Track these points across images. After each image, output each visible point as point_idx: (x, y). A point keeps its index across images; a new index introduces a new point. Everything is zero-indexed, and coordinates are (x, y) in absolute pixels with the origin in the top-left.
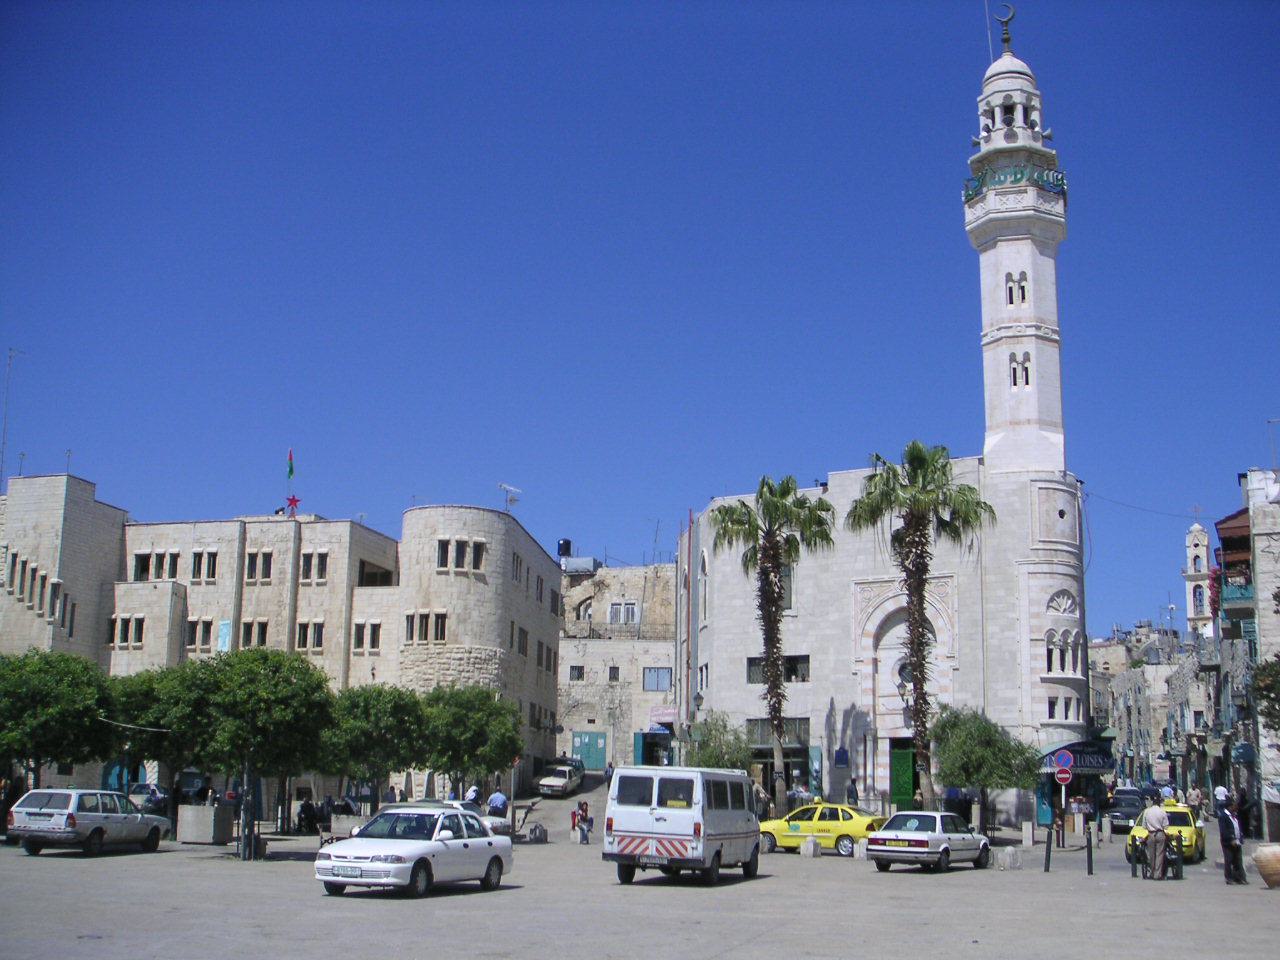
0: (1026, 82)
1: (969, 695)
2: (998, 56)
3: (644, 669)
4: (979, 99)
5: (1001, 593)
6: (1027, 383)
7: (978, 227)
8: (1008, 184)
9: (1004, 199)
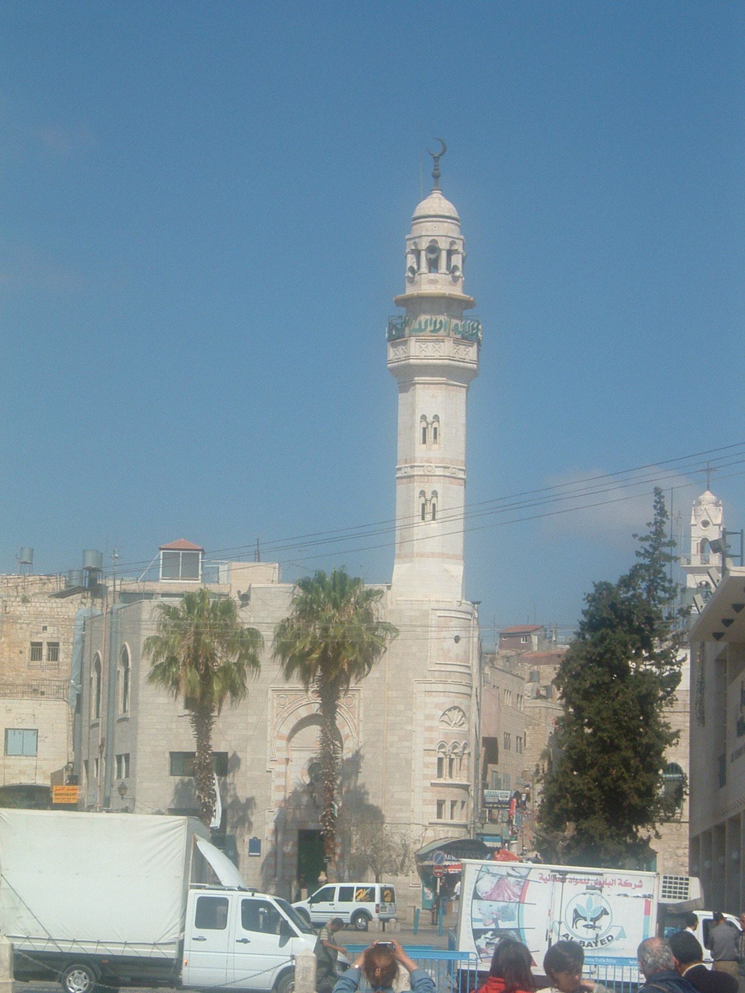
0: (453, 227)
2: (427, 194)
3: (7, 730)
4: (407, 237)
5: (401, 707)
7: (397, 368)
8: (427, 333)
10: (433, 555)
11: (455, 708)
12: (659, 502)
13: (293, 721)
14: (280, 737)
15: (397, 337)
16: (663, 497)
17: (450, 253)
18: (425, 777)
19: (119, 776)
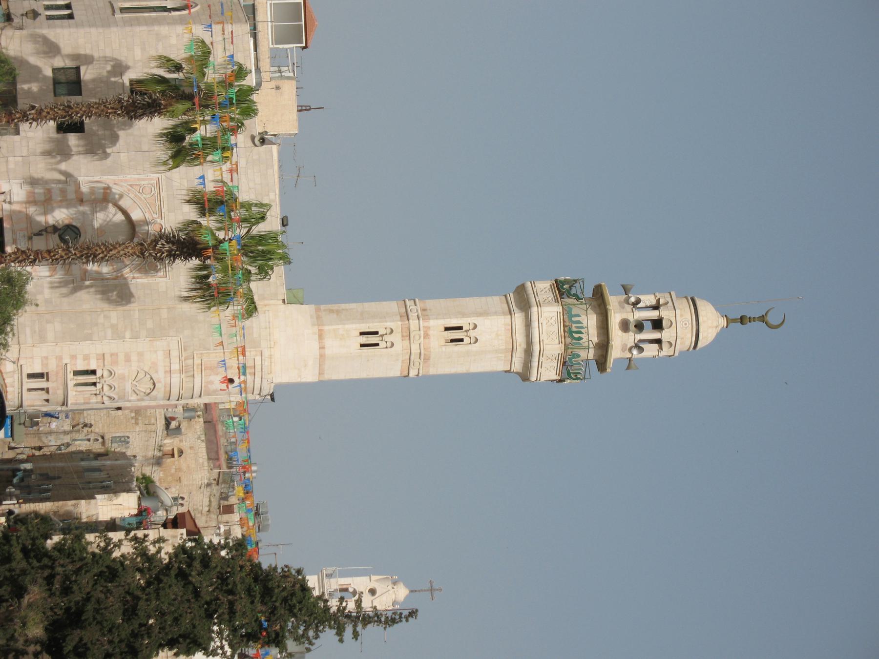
0: (688, 343)
5: (150, 324)
6: (362, 345)
9: (552, 321)
10: (322, 348)
11: (154, 384)
12: (401, 617)
15: (563, 290)
16: (407, 621)
17: (658, 341)
18: (74, 357)
19: (48, 8)
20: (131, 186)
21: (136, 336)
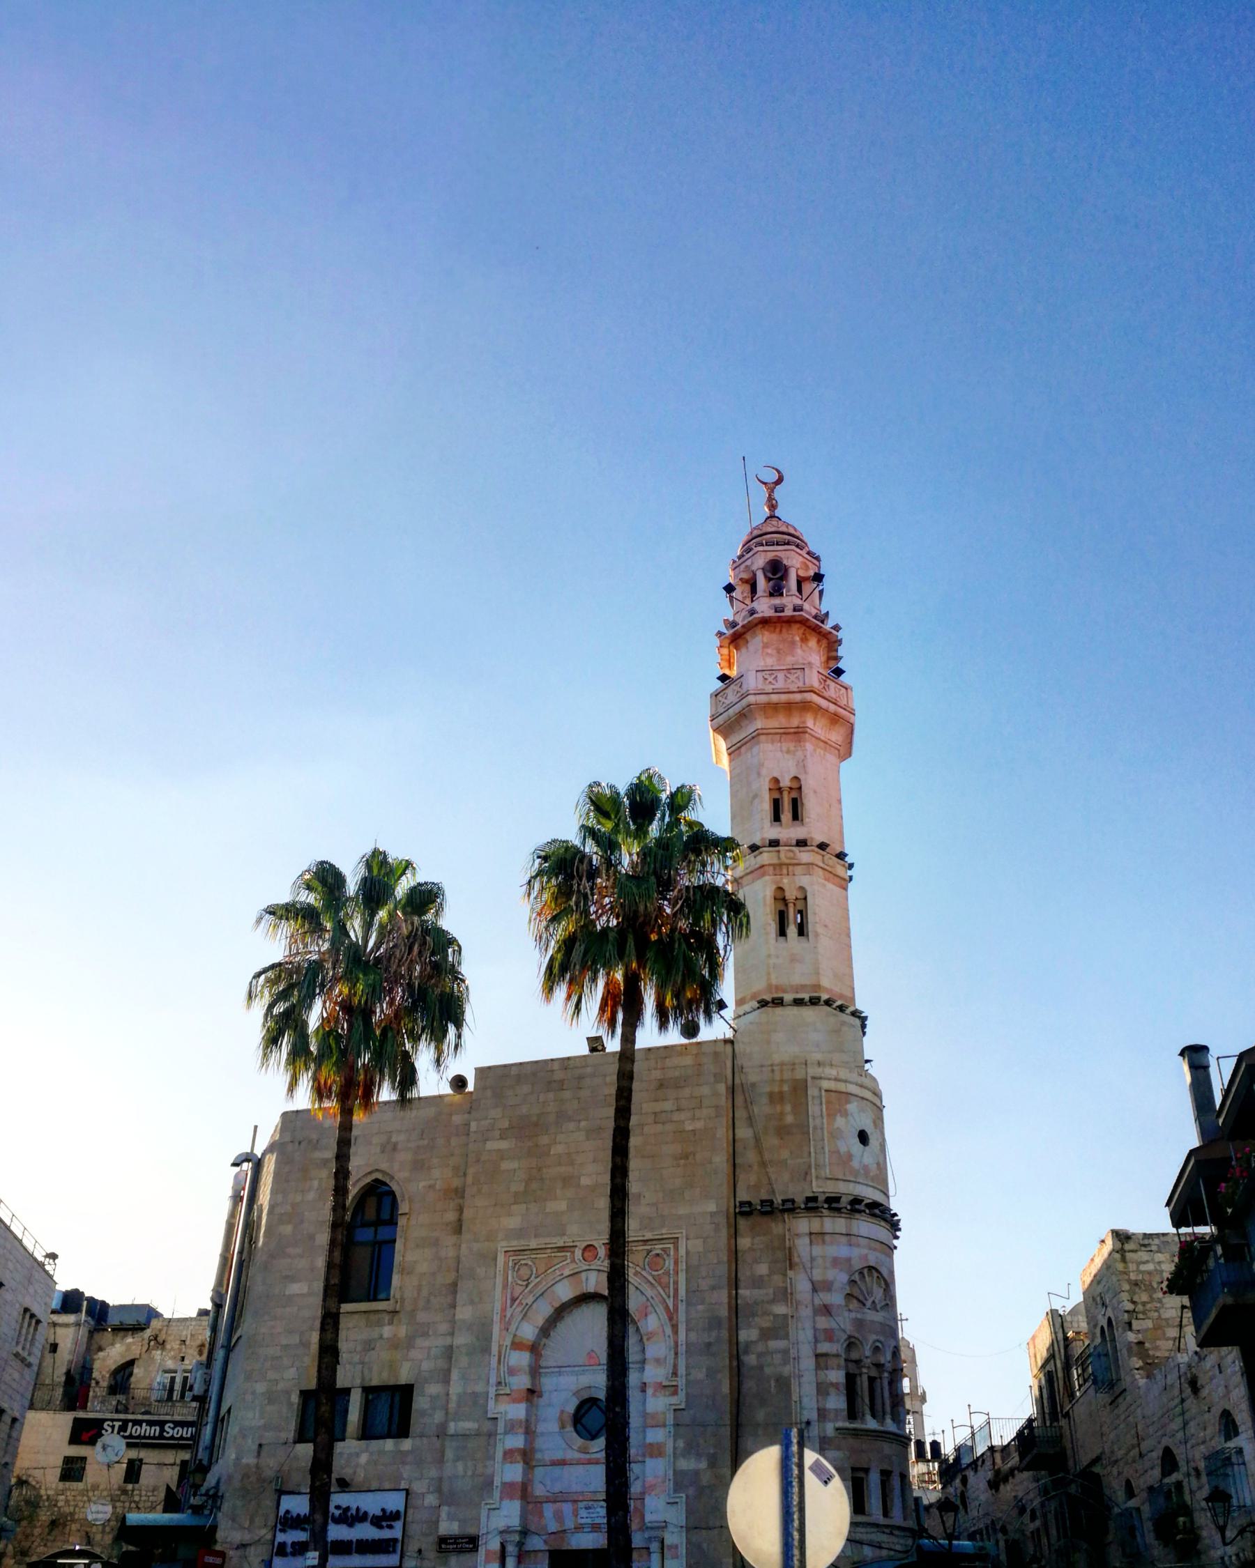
1: (703, 1465)
5: (762, 1269)
13: (544, 1311)
14: (517, 1345)
20: (514, 1300)
21: (785, 1295)
